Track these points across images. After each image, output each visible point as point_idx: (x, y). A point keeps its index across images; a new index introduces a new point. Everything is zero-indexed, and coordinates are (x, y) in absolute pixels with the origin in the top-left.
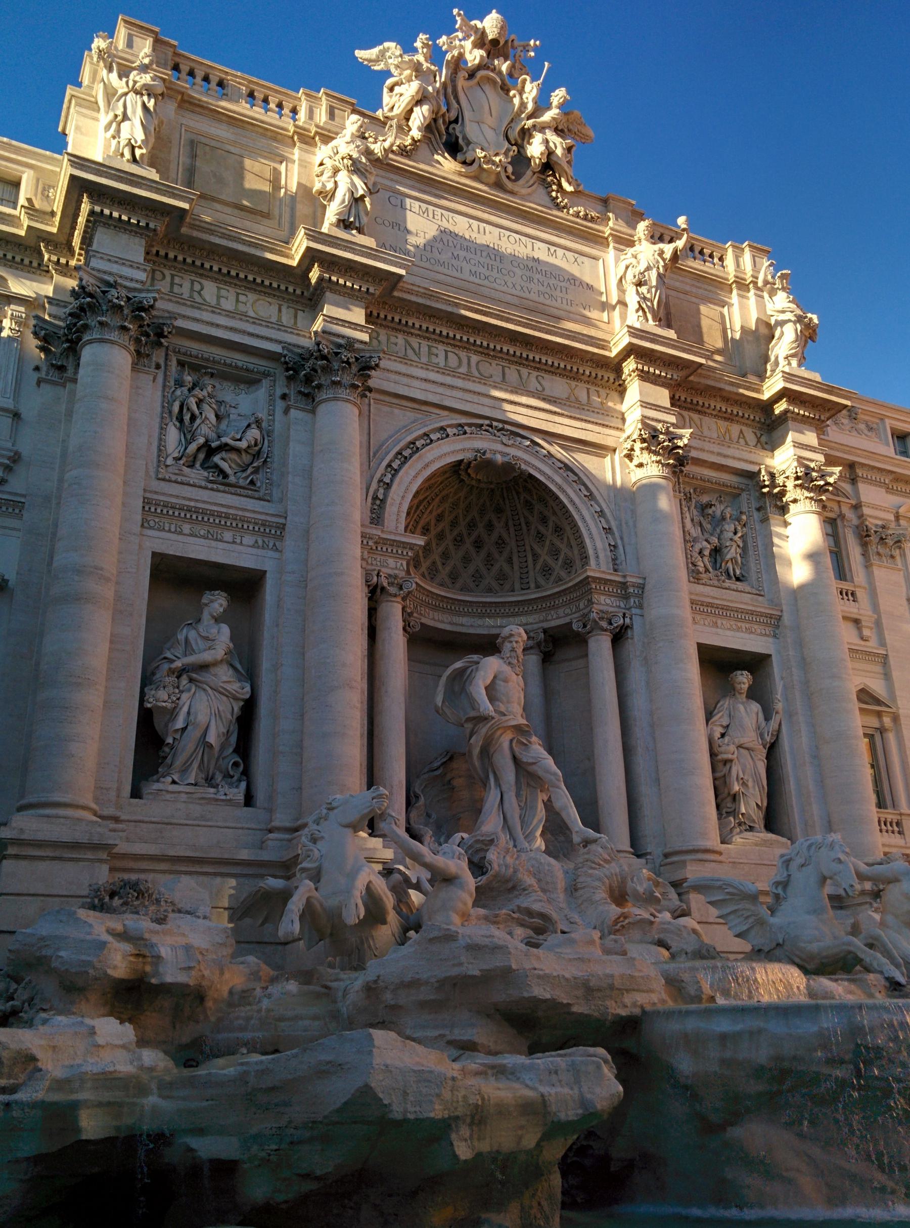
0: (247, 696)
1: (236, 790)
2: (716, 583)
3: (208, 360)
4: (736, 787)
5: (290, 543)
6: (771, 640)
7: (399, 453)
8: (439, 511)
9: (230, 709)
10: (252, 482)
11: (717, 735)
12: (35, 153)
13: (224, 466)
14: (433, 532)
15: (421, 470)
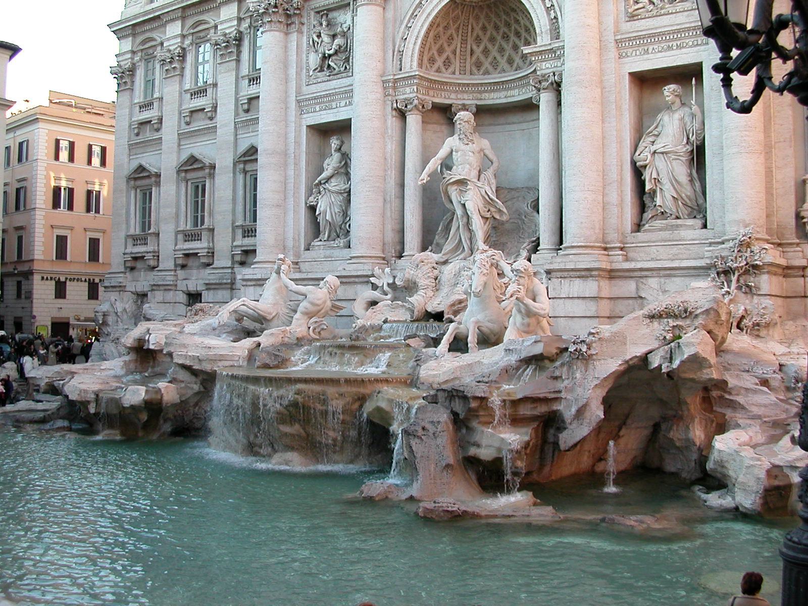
0: (348, 190)
1: (342, 241)
2: (654, 12)
3: (324, 6)
4: (648, 187)
5: (356, 99)
6: (702, 48)
7: (413, 14)
8: (480, 25)
9: (338, 200)
10: (346, 68)
11: (644, 145)
12: (144, 16)
13: (332, 64)
14: (485, 41)
15: (425, 20)
